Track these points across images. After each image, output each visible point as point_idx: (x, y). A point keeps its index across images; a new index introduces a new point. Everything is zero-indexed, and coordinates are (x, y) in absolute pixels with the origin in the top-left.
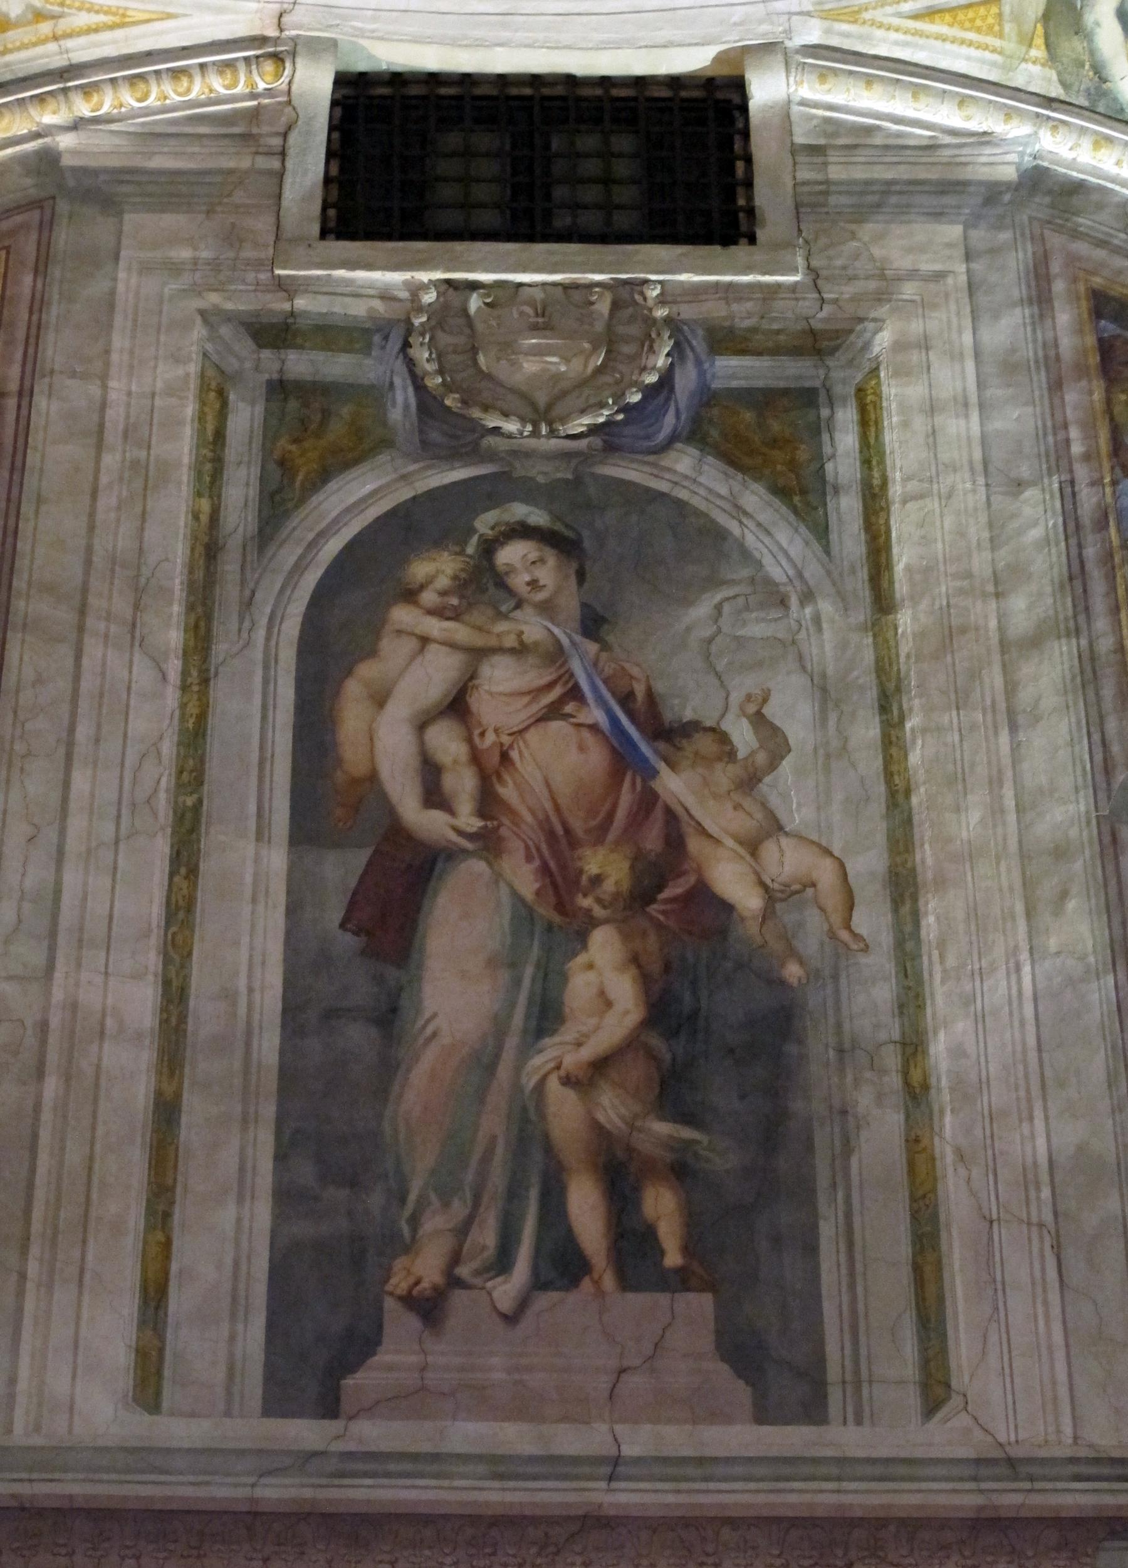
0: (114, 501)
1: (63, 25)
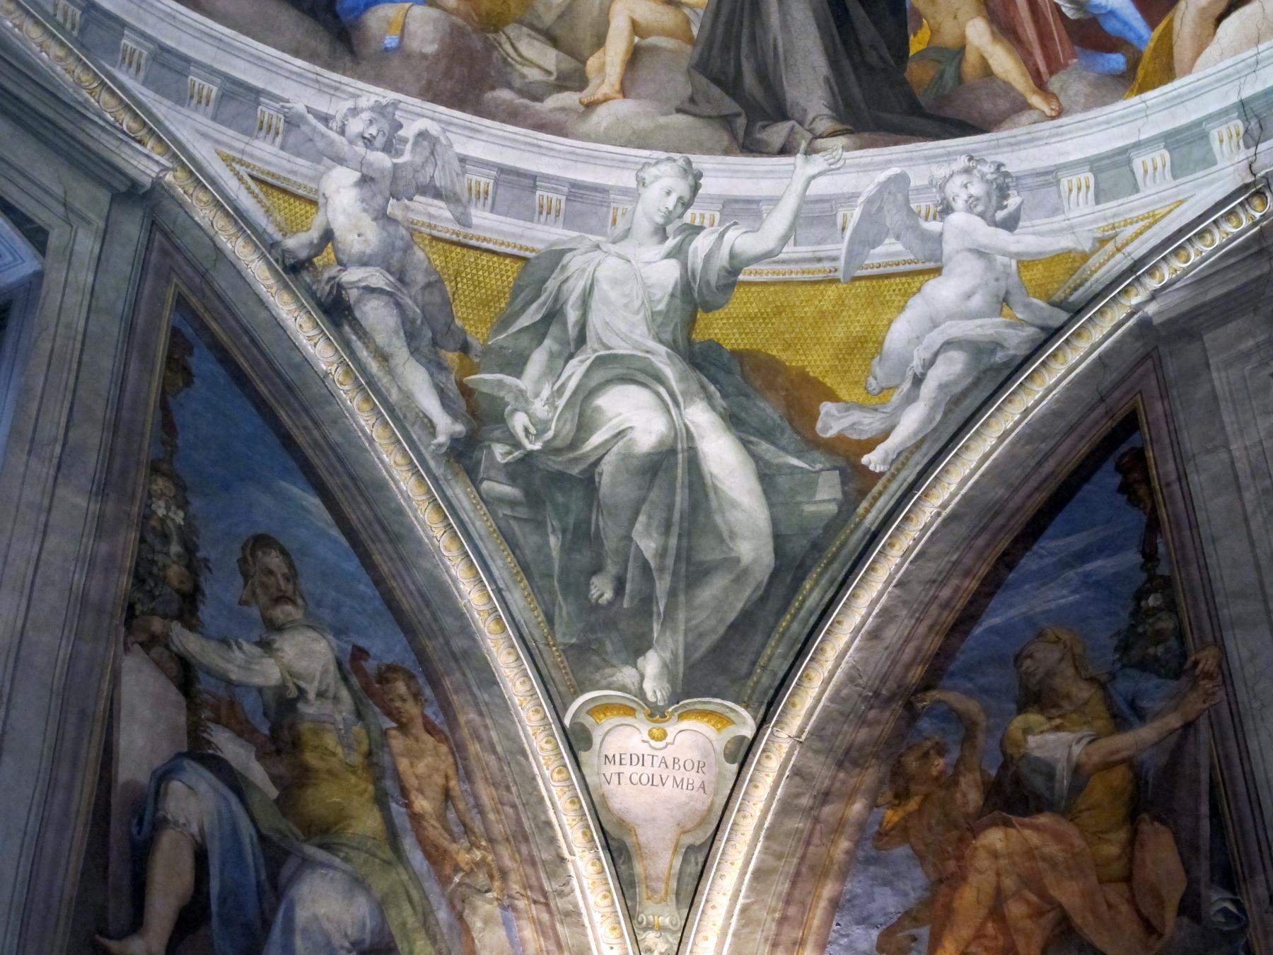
0: (1260, 518)
1: (1120, 240)
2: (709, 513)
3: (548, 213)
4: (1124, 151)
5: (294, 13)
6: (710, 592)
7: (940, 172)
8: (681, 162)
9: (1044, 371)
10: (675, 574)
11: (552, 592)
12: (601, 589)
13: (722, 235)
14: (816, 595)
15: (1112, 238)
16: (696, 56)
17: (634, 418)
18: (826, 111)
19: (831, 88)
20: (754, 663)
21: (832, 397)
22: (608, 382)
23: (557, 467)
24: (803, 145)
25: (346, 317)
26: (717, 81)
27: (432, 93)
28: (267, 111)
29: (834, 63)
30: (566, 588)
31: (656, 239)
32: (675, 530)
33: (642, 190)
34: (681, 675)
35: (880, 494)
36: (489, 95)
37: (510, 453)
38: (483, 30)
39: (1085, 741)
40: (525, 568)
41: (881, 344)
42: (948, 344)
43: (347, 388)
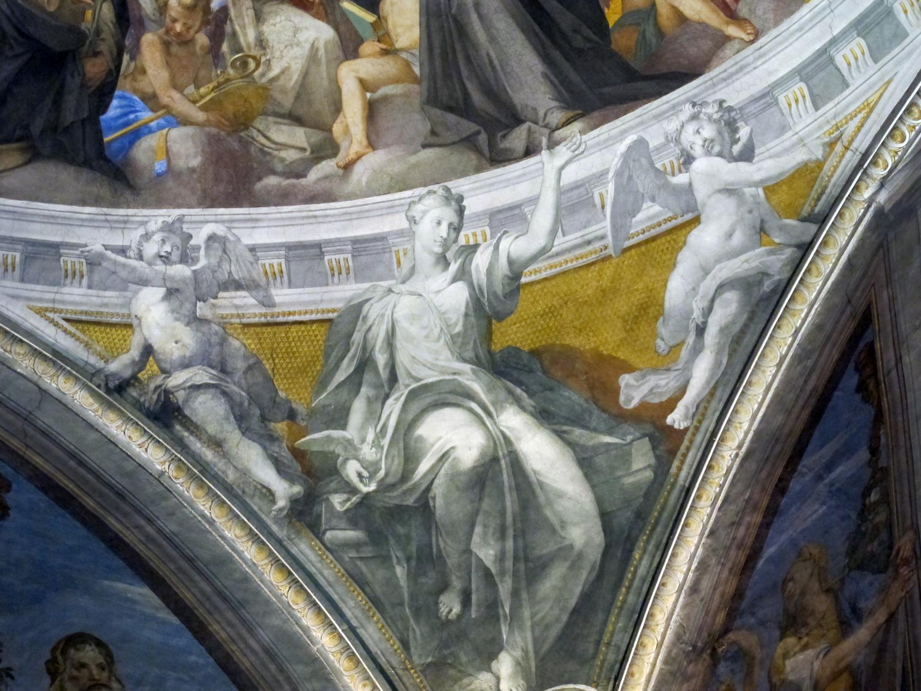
1: (846, 138)
2: (538, 508)
3: (340, 273)
4: (824, 51)
5: (72, 169)
6: (549, 585)
7: (672, 126)
8: (441, 192)
9: (802, 288)
10: (515, 574)
11: (404, 619)
12: (450, 605)
13: (497, 247)
14: (645, 562)
15: (839, 138)
16: (425, 94)
17: (455, 439)
18: (554, 104)
19: (552, 82)
20: (598, 643)
21: (628, 368)
22: (425, 411)
23: (396, 502)
24: (544, 141)
25: (176, 417)
26: (450, 109)
27: (210, 201)
28: (69, 260)
29: (546, 58)
30: (417, 612)
31: (439, 268)
32: (510, 532)
33: (415, 228)
34: (533, 669)
35: (688, 449)
36: (258, 186)
37: (348, 500)
38: (235, 131)
39: (821, 656)
40: (376, 602)
41: (662, 306)
42: (721, 288)
43: (181, 480)
